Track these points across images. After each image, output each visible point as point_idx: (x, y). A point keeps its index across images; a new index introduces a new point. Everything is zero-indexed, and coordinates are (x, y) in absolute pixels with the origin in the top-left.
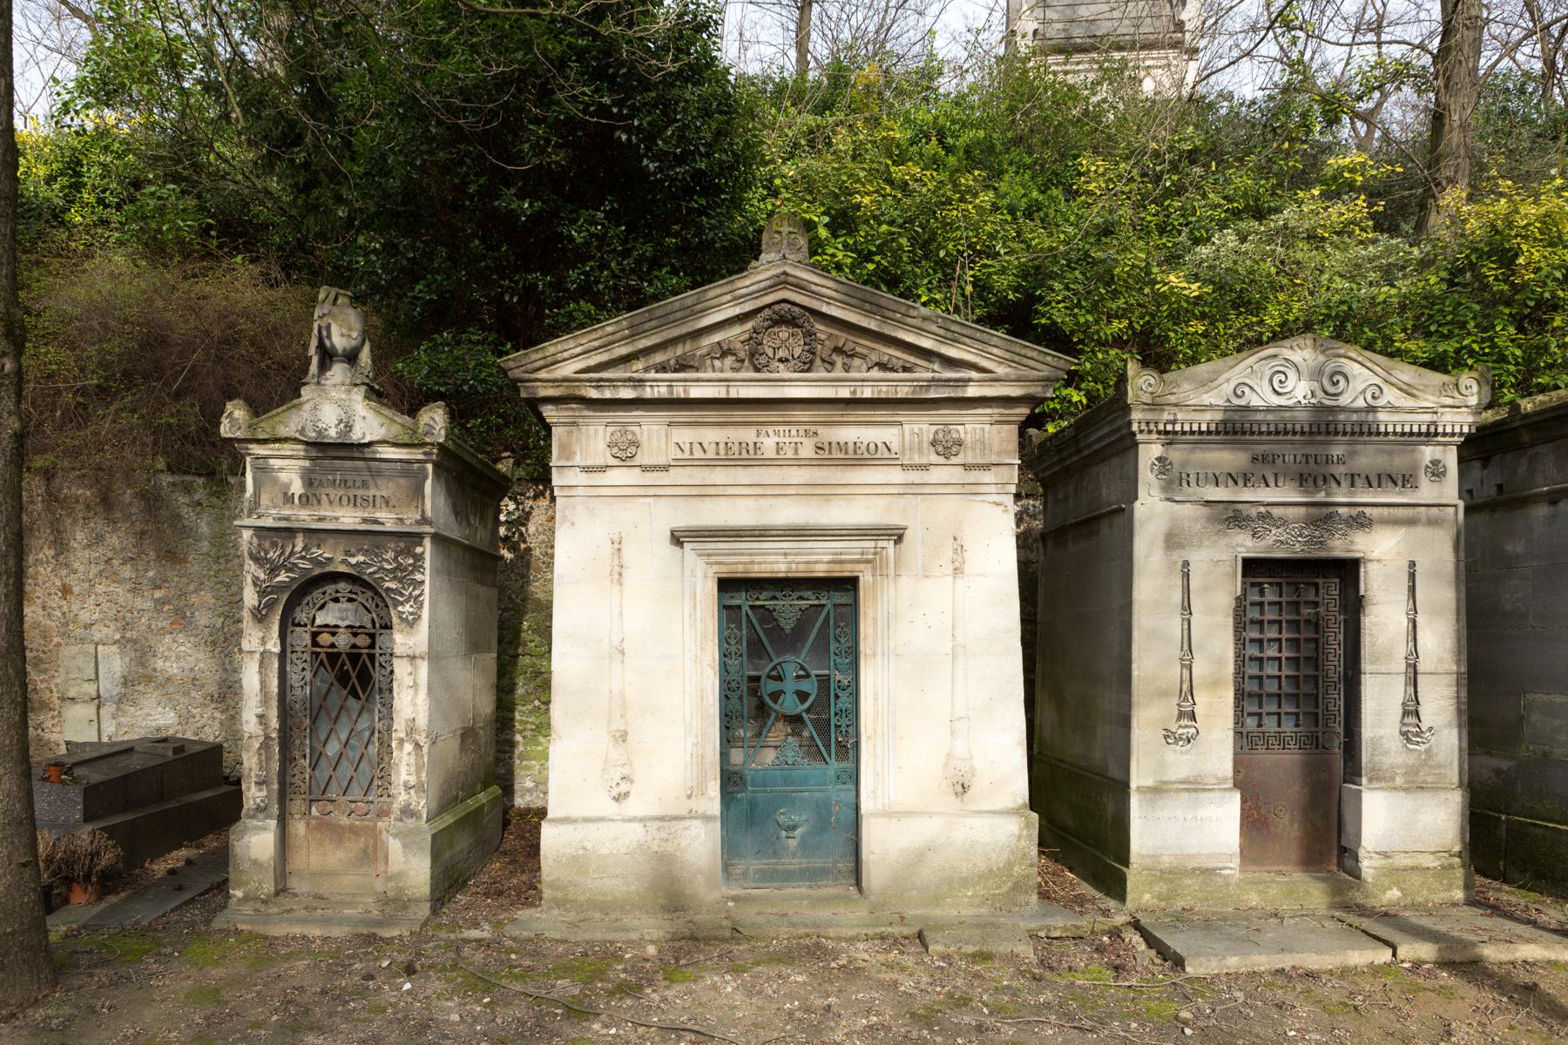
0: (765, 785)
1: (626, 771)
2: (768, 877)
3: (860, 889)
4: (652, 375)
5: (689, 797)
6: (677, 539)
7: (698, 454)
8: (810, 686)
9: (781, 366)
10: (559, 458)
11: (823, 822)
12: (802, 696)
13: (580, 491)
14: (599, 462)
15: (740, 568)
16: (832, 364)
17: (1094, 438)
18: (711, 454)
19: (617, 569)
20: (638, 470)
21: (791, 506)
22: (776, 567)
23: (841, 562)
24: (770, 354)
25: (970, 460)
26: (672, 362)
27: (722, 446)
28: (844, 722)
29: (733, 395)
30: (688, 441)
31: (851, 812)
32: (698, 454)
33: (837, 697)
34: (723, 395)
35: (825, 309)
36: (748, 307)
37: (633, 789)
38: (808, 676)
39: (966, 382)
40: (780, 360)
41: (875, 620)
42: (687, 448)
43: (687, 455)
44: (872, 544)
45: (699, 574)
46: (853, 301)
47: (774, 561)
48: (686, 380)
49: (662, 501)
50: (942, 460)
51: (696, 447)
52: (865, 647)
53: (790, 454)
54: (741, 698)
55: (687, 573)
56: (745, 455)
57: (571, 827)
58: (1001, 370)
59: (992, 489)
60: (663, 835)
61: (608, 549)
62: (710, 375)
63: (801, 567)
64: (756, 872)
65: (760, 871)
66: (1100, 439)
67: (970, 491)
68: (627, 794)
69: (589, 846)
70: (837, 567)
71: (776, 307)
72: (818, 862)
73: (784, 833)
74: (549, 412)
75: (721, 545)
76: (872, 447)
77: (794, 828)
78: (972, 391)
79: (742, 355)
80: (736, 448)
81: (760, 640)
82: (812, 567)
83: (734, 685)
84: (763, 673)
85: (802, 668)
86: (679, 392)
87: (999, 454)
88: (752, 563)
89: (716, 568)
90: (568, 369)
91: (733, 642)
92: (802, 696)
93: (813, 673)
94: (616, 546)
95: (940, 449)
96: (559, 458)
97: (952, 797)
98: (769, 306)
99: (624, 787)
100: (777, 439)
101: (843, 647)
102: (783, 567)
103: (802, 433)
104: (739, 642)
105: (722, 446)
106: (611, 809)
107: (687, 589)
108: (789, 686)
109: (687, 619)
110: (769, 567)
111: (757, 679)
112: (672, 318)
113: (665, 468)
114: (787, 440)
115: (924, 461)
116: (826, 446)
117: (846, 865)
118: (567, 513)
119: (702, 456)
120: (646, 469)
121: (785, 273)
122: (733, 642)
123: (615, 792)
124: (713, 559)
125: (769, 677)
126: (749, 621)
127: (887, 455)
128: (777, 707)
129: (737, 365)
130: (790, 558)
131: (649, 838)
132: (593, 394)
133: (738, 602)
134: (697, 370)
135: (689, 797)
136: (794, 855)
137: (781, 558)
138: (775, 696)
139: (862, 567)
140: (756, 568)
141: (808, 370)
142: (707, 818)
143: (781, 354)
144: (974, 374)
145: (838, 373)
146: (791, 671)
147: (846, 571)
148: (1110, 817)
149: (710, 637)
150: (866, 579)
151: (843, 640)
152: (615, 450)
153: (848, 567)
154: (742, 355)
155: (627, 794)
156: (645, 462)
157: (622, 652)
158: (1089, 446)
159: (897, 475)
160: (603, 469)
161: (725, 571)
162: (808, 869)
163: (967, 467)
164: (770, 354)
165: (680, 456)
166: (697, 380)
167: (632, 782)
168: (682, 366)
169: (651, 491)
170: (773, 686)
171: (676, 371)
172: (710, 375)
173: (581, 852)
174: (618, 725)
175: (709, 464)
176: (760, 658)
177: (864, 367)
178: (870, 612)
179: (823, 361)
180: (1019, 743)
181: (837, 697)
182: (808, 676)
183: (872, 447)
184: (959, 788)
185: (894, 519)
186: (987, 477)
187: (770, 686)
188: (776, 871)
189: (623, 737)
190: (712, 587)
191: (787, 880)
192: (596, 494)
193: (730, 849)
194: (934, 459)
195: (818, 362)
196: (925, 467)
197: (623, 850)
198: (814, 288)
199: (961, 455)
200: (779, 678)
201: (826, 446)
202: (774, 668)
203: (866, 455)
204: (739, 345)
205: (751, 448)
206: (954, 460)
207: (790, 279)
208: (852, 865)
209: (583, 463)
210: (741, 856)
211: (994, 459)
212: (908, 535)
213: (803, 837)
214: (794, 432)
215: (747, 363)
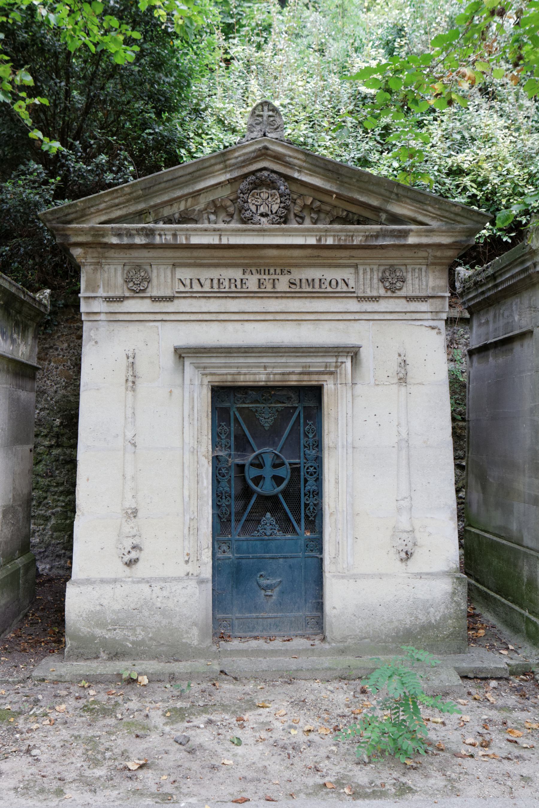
1: (136, 541)
4: (161, 225)
5: (187, 562)
6: (182, 354)
7: (196, 287)
9: (263, 220)
10: (86, 290)
12: (278, 480)
13: (103, 317)
14: (118, 293)
15: (229, 378)
16: (303, 218)
17: (508, 275)
18: (207, 288)
19: (131, 379)
20: (148, 301)
21: (267, 329)
22: (258, 378)
23: (309, 373)
24: (253, 208)
25: (410, 294)
26: (177, 216)
27: (215, 282)
28: (311, 501)
29: (224, 241)
30: (189, 277)
32: (196, 287)
34: (216, 241)
35: (296, 175)
36: (236, 174)
37: (142, 556)
38: (283, 464)
39: (405, 234)
40: (262, 215)
41: (337, 419)
42: (188, 282)
43: (188, 289)
44: (334, 360)
45: (197, 382)
46: (318, 170)
47: (258, 373)
48: (187, 230)
49: (168, 324)
50: (389, 294)
51: (195, 282)
52: (328, 440)
53: (269, 289)
54: (229, 481)
55: (187, 381)
56: (233, 289)
57: (90, 588)
58: (435, 224)
59: (428, 316)
60: (165, 593)
61: (124, 363)
62: (206, 225)
63: (278, 377)
66: (512, 277)
67: (412, 317)
68: (136, 561)
69: (105, 602)
70: (306, 378)
71: (258, 174)
74: (77, 252)
75: (214, 360)
76: (334, 283)
78: (411, 240)
79: (231, 210)
80: (226, 283)
81: (245, 435)
82: (286, 377)
83: (224, 471)
86: (182, 240)
87: (433, 288)
88: (239, 374)
89: (209, 378)
90: (93, 223)
91: (223, 437)
92: (278, 480)
93: (287, 461)
94: (131, 360)
95: (387, 284)
96: (86, 290)
97: (399, 563)
98: (253, 173)
99: (134, 555)
100: (259, 276)
101: (311, 441)
102: (263, 377)
103: (278, 271)
104: (229, 437)
105: (215, 282)
106: (121, 571)
107: (187, 395)
108: (268, 472)
109: (186, 419)
110: (252, 378)
112: (176, 181)
113: (170, 299)
114: (267, 277)
115: (375, 294)
116: (298, 282)
118: (92, 333)
119: (200, 289)
120: (156, 299)
121: (266, 148)
122: (223, 437)
123: (127, 558)
124: (208, 371)
125: (252, 464)
126: (236, 419)
127: (345, 289)
128: (258, 489)
129: (228, 219)
130: (269, 370)
131: (154, 596)
132: (115, 240)
133: (227, 405)
134: (196, 222)
135: (187, 562)
137: (262, 370)
138: (258, 480)
139: (326, 377)
140: (242, 378)
141: (285, 222)
142: (201, 582)
143: (262, 210)
144: (413, 227)
145: (308, 225)
147: (313, 380)
148: (525, 580)
149: (205, 432)
150: (329, 387)
151: (311, 436)
152: (131, 284)
153: (315, 377)
154: (231, 210)
155: (136, 561)
156: (155, 293)
157: (134, 445)
158: (502, 283)
159: (353, 305)
160: (121, 299)
161: (217, 380)
163: (409, 299)
164: (253, 208)
165: (182, 289)
166: (195, 230)
167: (141, 549)
168: (185, 218)
169: (159, 317)
171: (179, 222)
172: (206, 225)
173: (98, 608)
174: (130, 503)
175: (206, 296)
177: (328, 220)
178: (332, 413)
179: (296, 215)
180: (451, 519)
181: (306, 481)
183: (334, 283)
184: (403, 555)
185: (351, 340)
186: (424, 306)
187: (251, 473)
189: (135, 513)
190: (206, 395)
192: (114, 319)
194: (382, 292)
195: (292, 216)
196: (376, 299)
197: (133, 606)
198: (288, 159)
199: (404, 289)
200: (260, 466)
201: (298, 282)
202: (257, 457)
203: (329, 289)
204: (229, 203)
205: (238, 283)
206: (398, 293)
207: (269, 152)
209: (105, 295)
211: (430, 293)
212: (363, 353)
214: (272, 271)
215: (235, 217)
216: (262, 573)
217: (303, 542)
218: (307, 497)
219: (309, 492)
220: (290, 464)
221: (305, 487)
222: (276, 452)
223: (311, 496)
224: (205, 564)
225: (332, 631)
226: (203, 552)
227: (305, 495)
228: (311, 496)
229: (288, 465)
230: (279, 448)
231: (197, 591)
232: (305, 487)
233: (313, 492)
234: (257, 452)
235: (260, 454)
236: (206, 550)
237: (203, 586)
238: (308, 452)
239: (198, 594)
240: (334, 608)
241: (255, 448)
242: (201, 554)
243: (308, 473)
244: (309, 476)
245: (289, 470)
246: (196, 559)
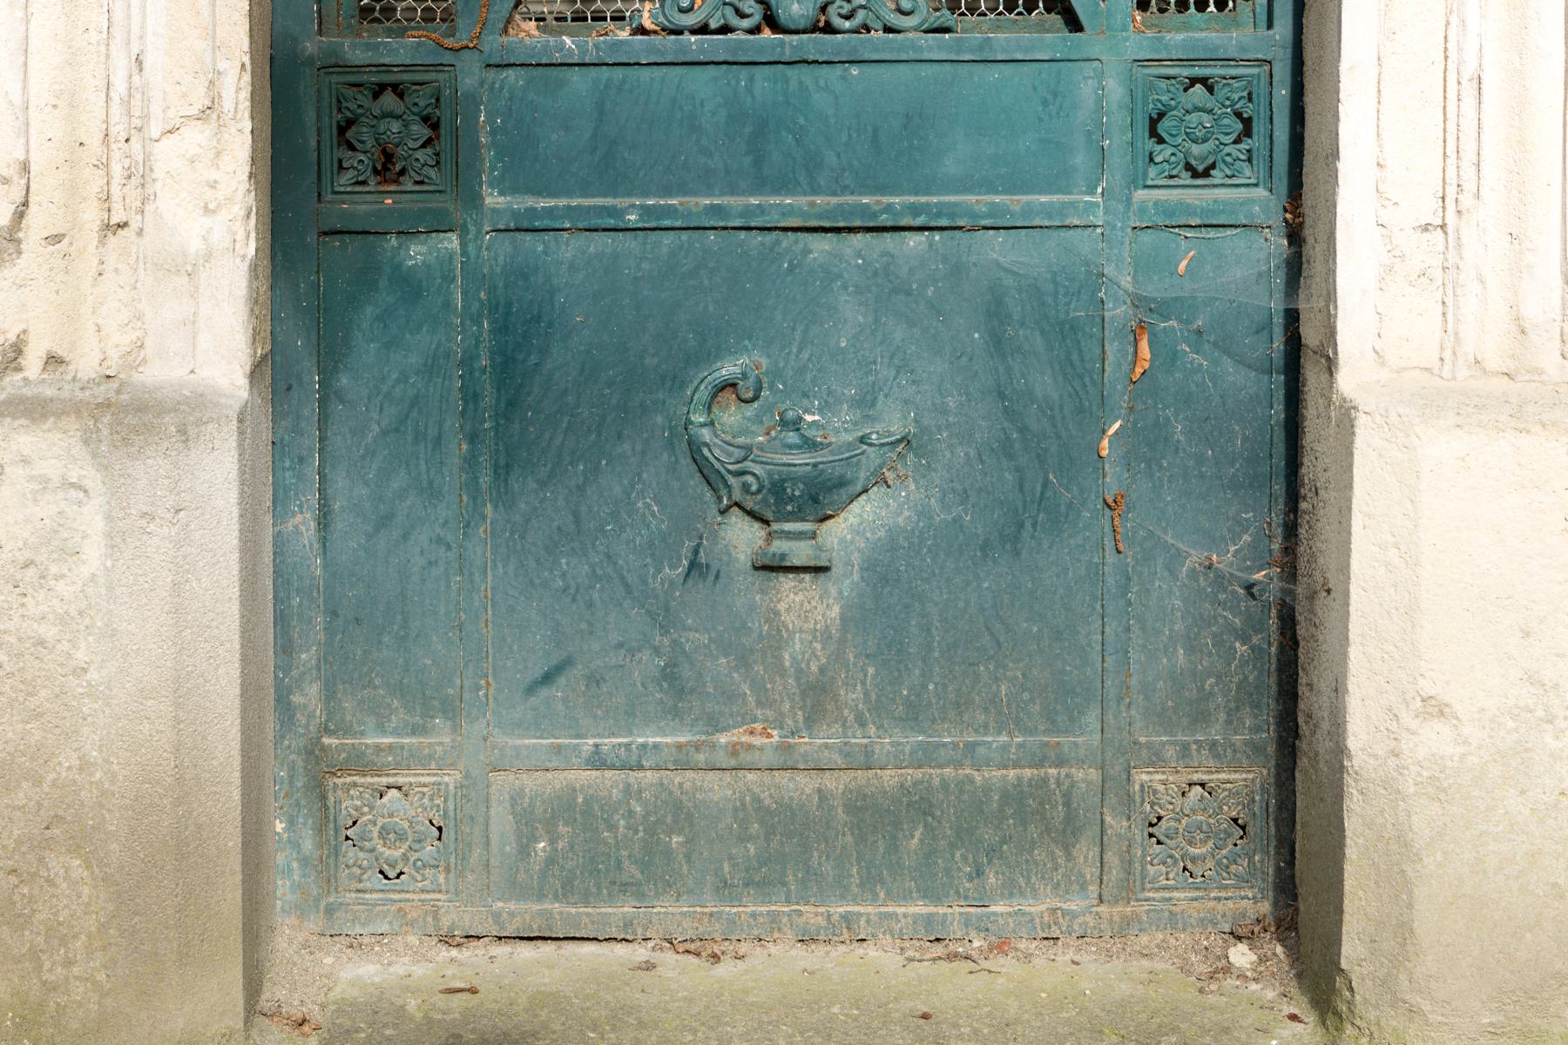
0: (609, 172)
2: (599, 862)
3: (1320, 981)
11: (1029, 486)
31: (1248, 384)
64: (528, 822)
65: (566, 808)
72: (995, 760)
73: (742, 538)
77: (817, 497)
117: (1203, 778)
136: (817, 699)
162: (920, 804)
188: (680, 813)
191: (761, 879)
193: (327, 641)
208: (1243, 780)
210: (431, 701)
213: (885, 570)
216: (728, 369)
217: (1115, 90)
224: (188, 270)
225: (1405, 931)
226: (168, 154)
231: (91, 519)
236: (196, 137)
237: (151, 470)
239: (94, 555)
240: (1436, 709)
242: (141, 176)
246: (92, 216)
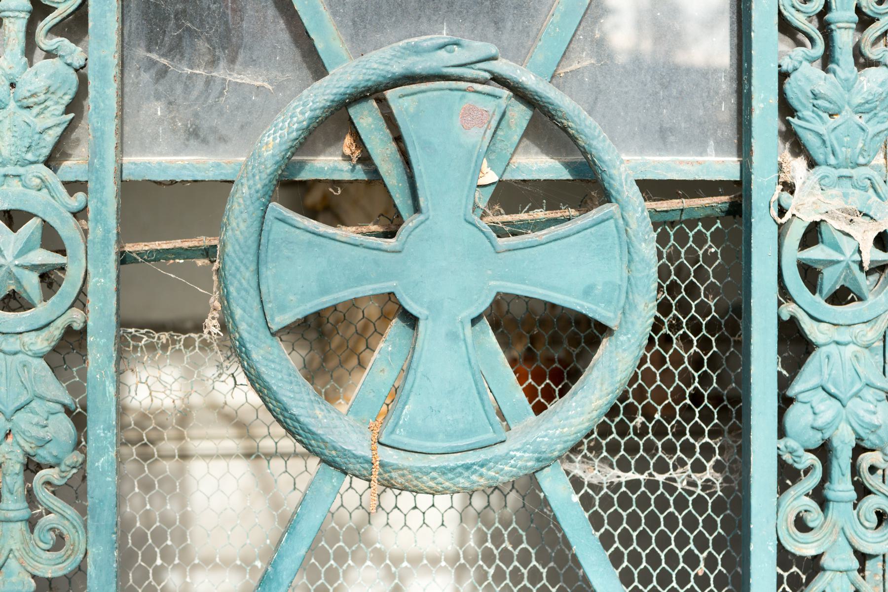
8: (608, 270)
12: (547, 345)
33: (795, 344)
38: (585, 188)
84: (247, 160)
85: (547, 126)
93: (625, 165)
111: (204, 199)
146: (460, 145)
170: (319, 265)
176: (228, 45)
181: (795, 344)
182: (585, 188)
200: (369, 204)
202: (335, 122)
218: (798, 499)
219: (824, 451)
220: (652, 189)
221: (785, 402)
222: (529, 79)
223: (841, 488)
227: (787, 475)
228: (841, 488)
229: (633, 194)
230: (545, 51)
232: (785, 402)
233: (859, 450)
234: (346, 73)
235: (374, 93)
238: (808, 78)
241: (328, 37)
243: (810, 274)
244: (817, 303)
245: (647, 248)
